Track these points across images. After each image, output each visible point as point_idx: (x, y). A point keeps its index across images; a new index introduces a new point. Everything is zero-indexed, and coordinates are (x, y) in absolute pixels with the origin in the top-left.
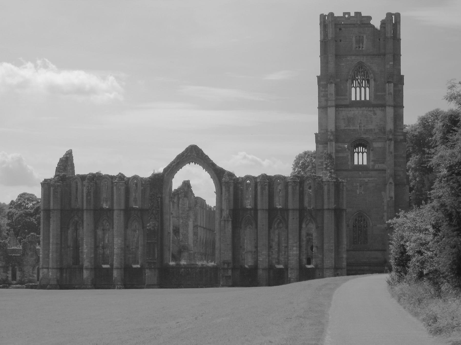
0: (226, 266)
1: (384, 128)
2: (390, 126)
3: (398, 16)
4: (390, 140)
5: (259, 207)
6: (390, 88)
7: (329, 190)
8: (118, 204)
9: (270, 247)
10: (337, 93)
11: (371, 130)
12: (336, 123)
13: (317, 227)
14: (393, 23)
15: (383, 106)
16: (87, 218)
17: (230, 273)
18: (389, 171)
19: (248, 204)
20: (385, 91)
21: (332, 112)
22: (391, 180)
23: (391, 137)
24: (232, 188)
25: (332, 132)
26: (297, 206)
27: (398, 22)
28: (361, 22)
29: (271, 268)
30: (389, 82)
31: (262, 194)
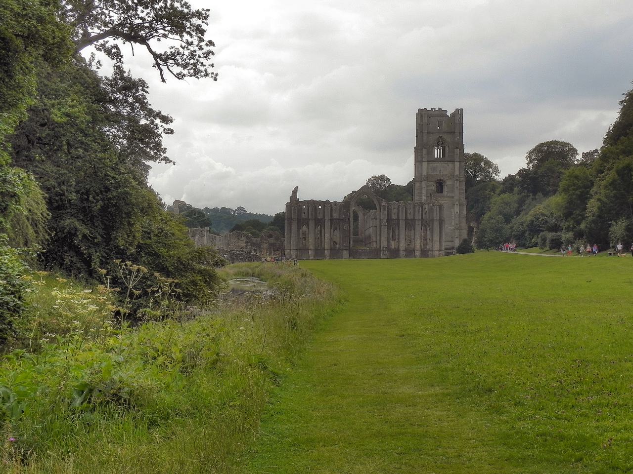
0: (385, 249)
3: (462, 110)
5: (400, 218)
6: (457, 151)
10: (428, 153)
13: (430, 229)
15: (453, 161)
16: (312, 224)
19: (394, 217)
21: (425, 164)
22: (457, 203)
25: (425, 176)
27: (461, 114)
28: (441, 113)
29: (406, 250)
30: (457, 148)
31: (402, 211)
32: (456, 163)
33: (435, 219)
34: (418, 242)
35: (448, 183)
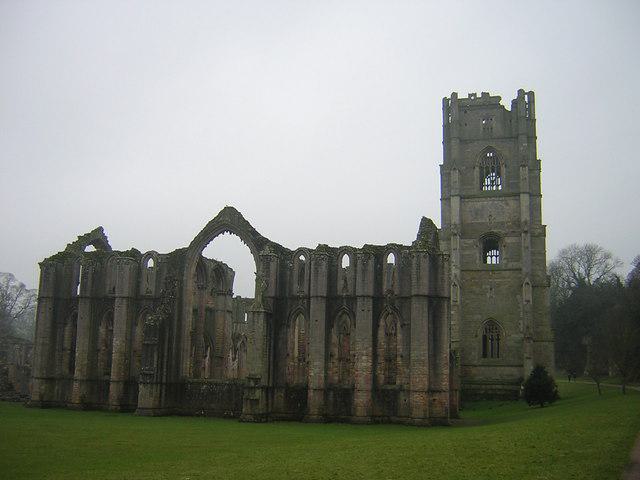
0: (252, 384)
1: (519, 220)
2: (525, 216)
3: (531, 94)
4: (526, 232)
6: (524, 172)
7: (419, 266)
8: (124, 289)
9: (328, 356)
11: (503, 223)
12: (461, 216)
14: (525, 103)
17: (258, 394)
18: (524, 269)
20: (518, 177)
21: (455, 202)
22: (527, 280)
23: (526, 229)
24: (273, 266)
26: (370, 291)
27: (532, 101)
28: (489, 103)
29: (328, 389)
32: (522, 195)
33: (414, 292)
34: (364, 363)
35: (508, 240)
